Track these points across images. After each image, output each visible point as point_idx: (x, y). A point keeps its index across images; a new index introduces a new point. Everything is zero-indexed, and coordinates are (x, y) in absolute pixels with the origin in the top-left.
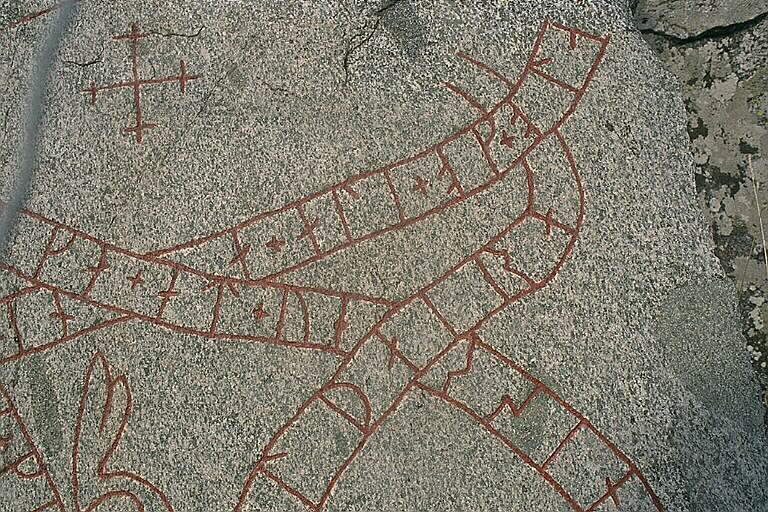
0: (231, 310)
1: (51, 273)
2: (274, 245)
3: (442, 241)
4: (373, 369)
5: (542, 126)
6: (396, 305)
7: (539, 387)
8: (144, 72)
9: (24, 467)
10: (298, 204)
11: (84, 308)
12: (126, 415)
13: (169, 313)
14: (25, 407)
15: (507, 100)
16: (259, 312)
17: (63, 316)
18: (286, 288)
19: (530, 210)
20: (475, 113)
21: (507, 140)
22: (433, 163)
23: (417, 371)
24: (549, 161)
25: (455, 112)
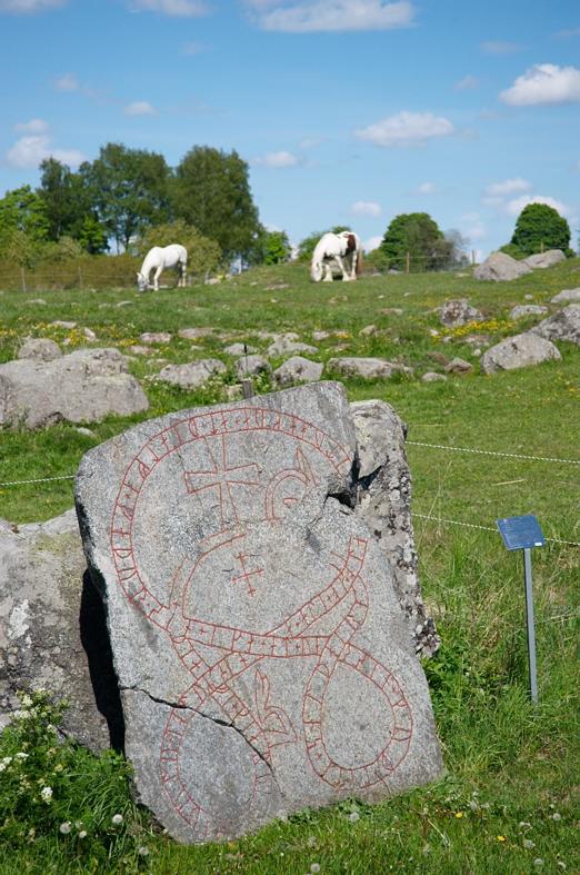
0: (291, 648)
1: (237, 647)
2: (297, 624)
3: (336, 616)
4: (326, 657)
5: (355, 574)
6: (329, 637)
7: (367, 654)
8: (248, 571)
9: (243, 713)
10: (299, 610)
11: (250, 657)
12: (269, 689)
13: (275, 653)
14: (239, 694)
15: (345, 566)
16: (297, 647)
17: (243, 660)
18: (303, 638)
19: (356, 602)
20: (338, 573)
21: (348, 580)
22: (330, 591)
23: (338, 656)
24: (358, 586)
25: (334, 573)
